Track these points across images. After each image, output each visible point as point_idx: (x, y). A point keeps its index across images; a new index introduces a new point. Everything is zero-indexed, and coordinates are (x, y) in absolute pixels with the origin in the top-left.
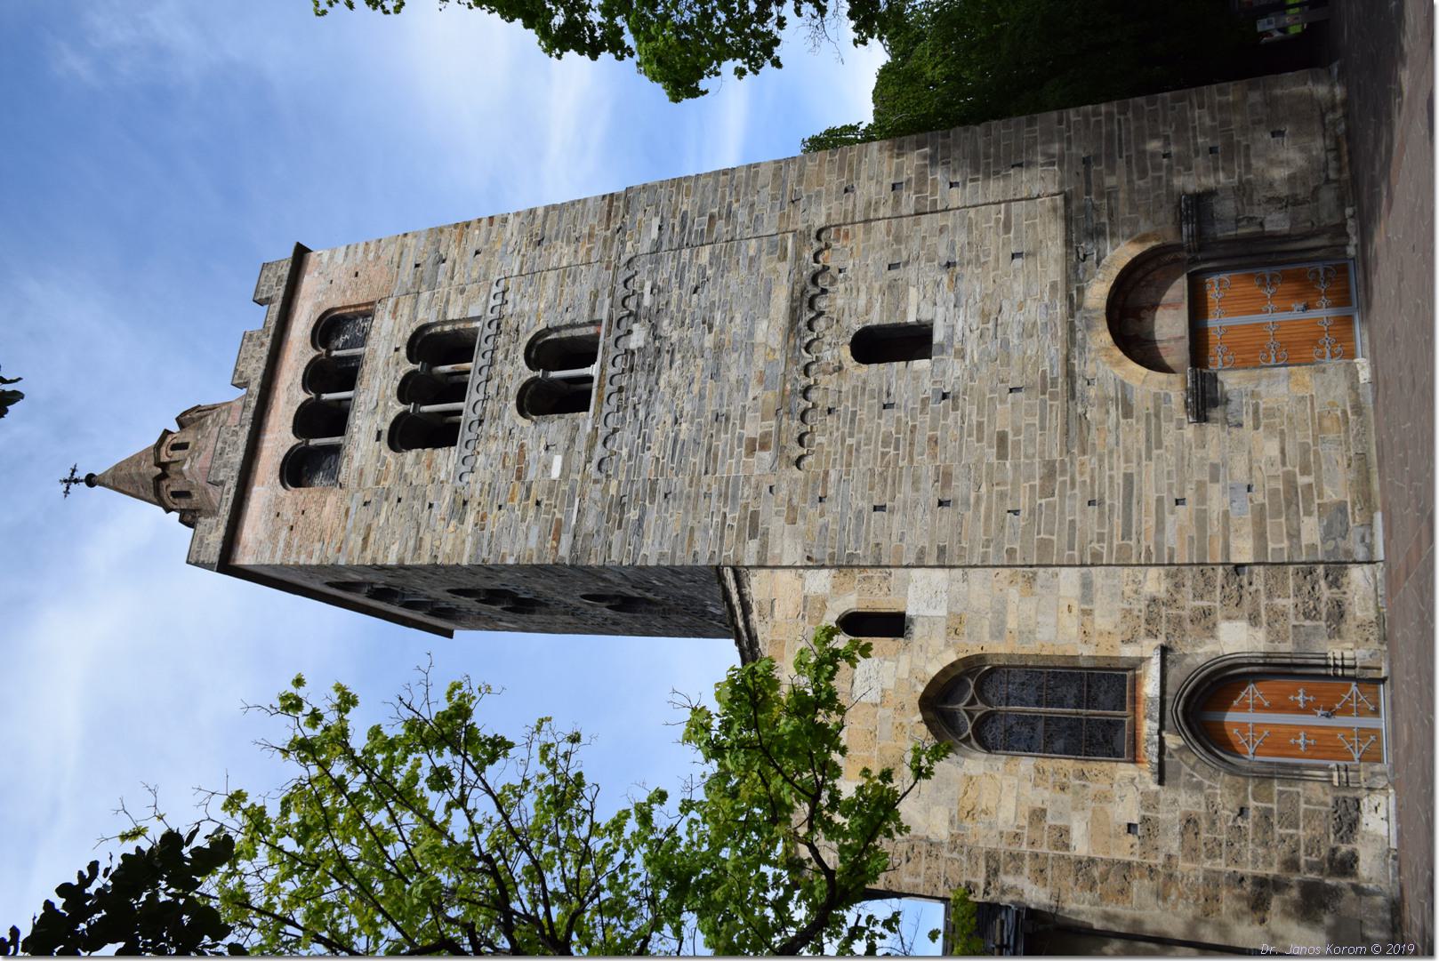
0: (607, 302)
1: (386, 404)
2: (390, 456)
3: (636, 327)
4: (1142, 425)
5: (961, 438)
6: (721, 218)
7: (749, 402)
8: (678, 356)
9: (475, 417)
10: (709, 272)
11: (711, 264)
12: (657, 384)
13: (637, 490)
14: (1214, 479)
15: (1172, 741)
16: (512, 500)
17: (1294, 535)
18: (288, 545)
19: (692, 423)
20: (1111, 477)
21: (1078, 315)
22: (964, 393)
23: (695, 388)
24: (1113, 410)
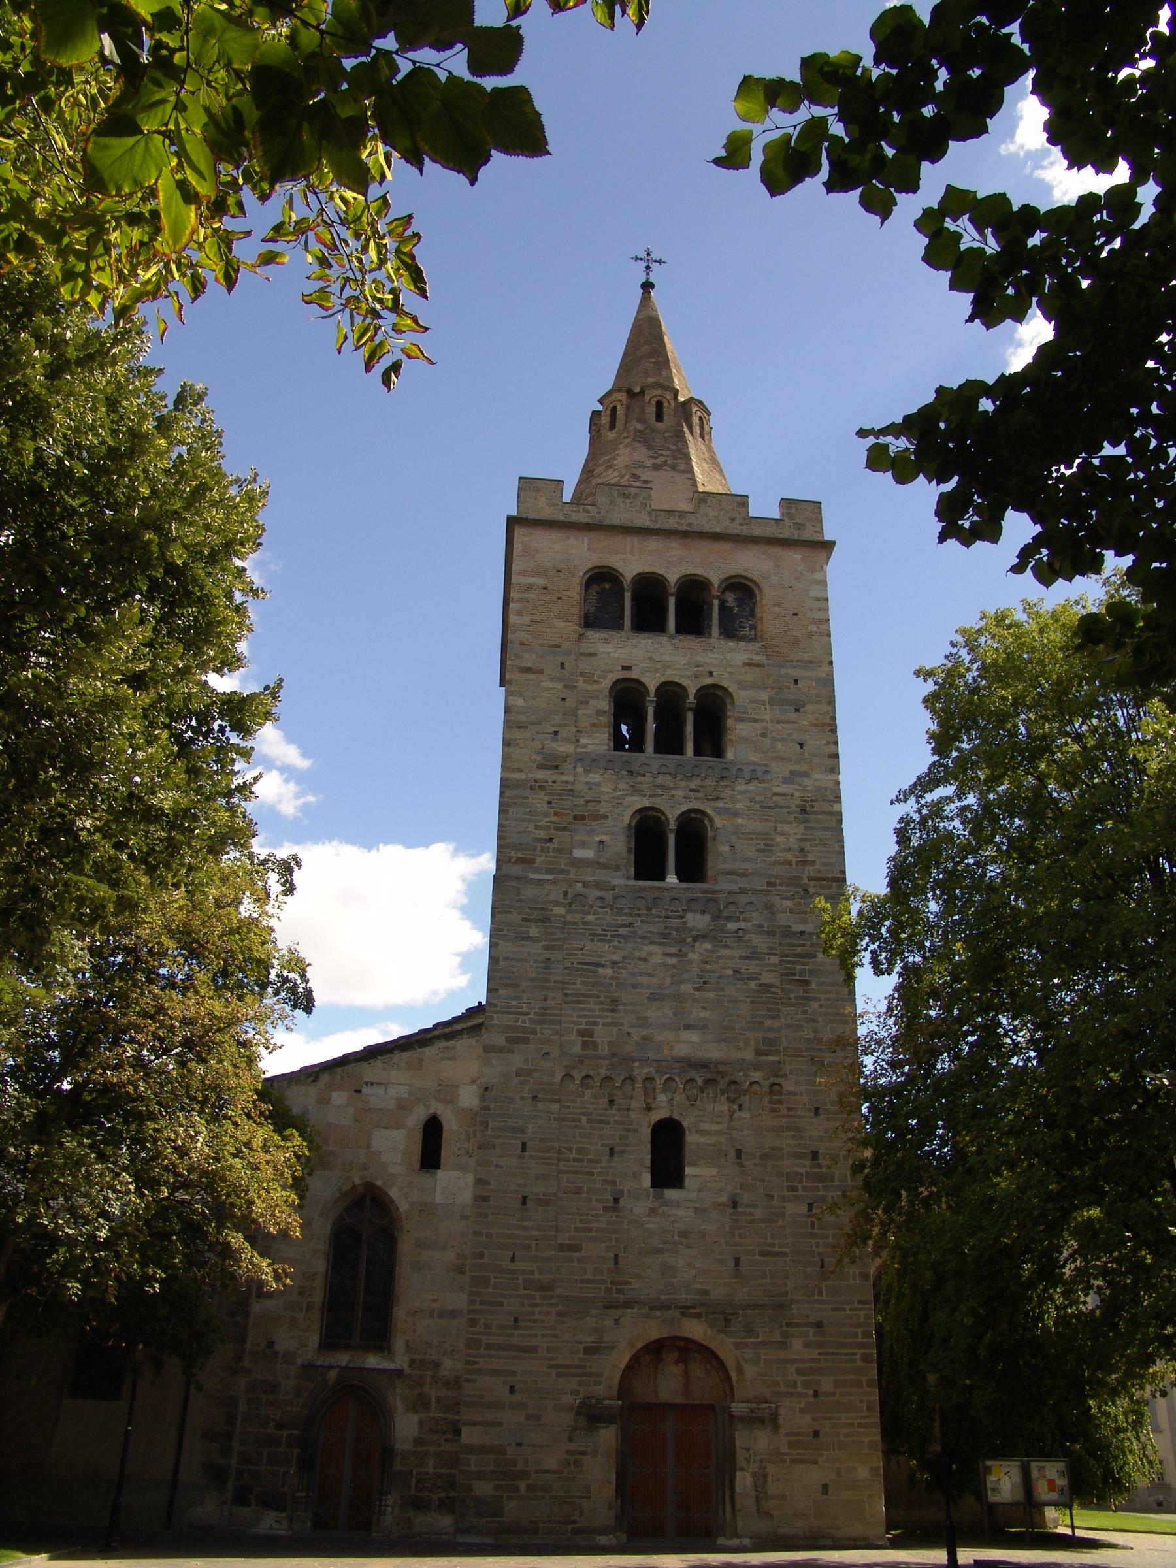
0: (735, 887)
1: (657, 670)
2: (606, 683)
3: (707, 917)
4: (577, 1362)
5: (580, 1215)
6: (805, 991)
7: (626, 1028)
8: (674, 961)
9: (635, 767)
10: (752, 984)
11: (761, 985)
12: (651, 943)
13: (554, 933)
14: (528, 1417)
15: (332, 1375)
16: (556, 814)
17: (480, 1476)
18: (529, 588)
19: (612, 978)
20: (536, 1336)
21: (677, 1314)
22: (617, 1216)
23: (642, 979)
24: (592, 1339)
